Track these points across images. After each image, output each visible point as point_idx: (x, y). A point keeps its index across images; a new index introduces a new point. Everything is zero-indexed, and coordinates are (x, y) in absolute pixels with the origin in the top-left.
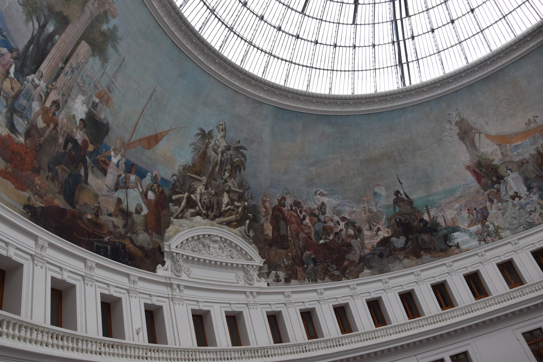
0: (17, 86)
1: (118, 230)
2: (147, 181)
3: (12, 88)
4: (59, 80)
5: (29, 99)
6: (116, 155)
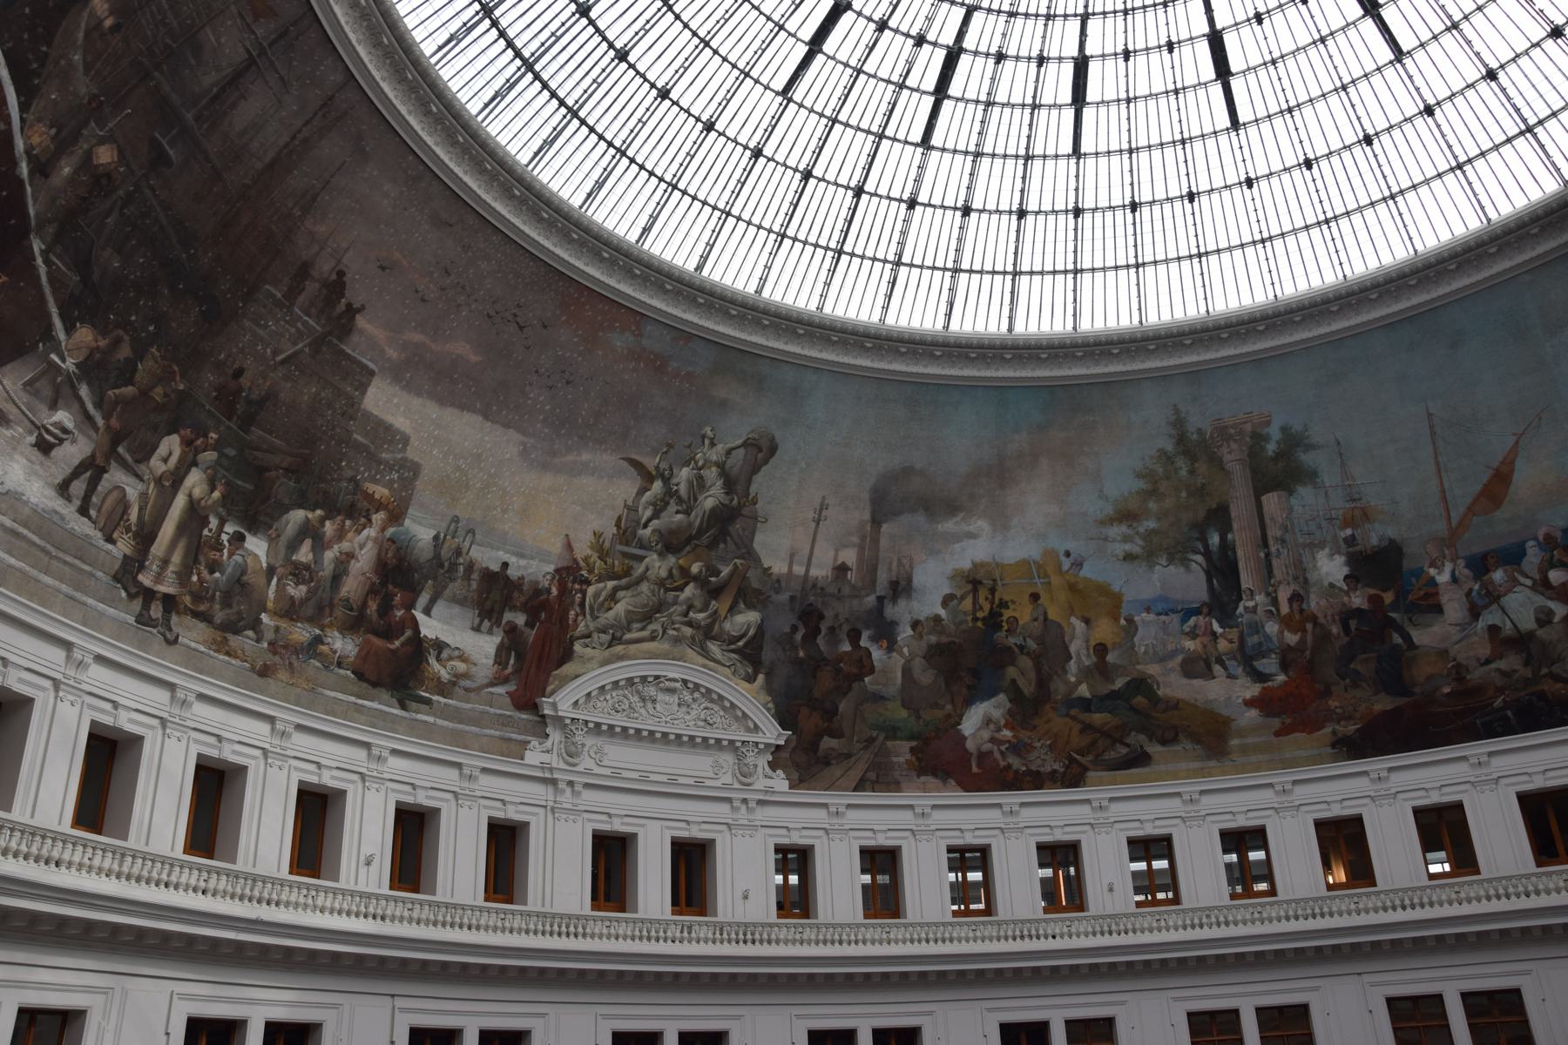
0: (1234, 634)
1: (1516, 676)
2: (1533, 556)
3: (1231, 642)
4: (1276, 572)
5: (1257, 628)
6: (1440, 570)
